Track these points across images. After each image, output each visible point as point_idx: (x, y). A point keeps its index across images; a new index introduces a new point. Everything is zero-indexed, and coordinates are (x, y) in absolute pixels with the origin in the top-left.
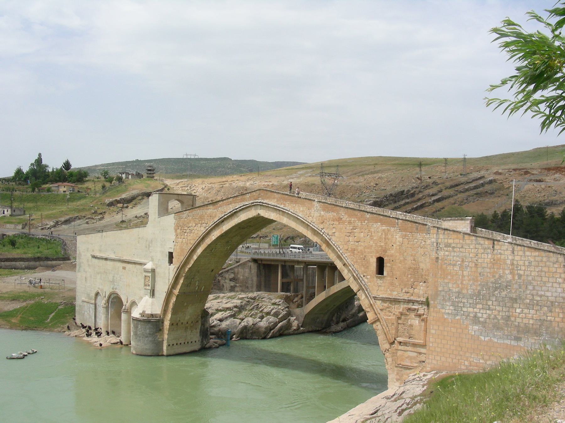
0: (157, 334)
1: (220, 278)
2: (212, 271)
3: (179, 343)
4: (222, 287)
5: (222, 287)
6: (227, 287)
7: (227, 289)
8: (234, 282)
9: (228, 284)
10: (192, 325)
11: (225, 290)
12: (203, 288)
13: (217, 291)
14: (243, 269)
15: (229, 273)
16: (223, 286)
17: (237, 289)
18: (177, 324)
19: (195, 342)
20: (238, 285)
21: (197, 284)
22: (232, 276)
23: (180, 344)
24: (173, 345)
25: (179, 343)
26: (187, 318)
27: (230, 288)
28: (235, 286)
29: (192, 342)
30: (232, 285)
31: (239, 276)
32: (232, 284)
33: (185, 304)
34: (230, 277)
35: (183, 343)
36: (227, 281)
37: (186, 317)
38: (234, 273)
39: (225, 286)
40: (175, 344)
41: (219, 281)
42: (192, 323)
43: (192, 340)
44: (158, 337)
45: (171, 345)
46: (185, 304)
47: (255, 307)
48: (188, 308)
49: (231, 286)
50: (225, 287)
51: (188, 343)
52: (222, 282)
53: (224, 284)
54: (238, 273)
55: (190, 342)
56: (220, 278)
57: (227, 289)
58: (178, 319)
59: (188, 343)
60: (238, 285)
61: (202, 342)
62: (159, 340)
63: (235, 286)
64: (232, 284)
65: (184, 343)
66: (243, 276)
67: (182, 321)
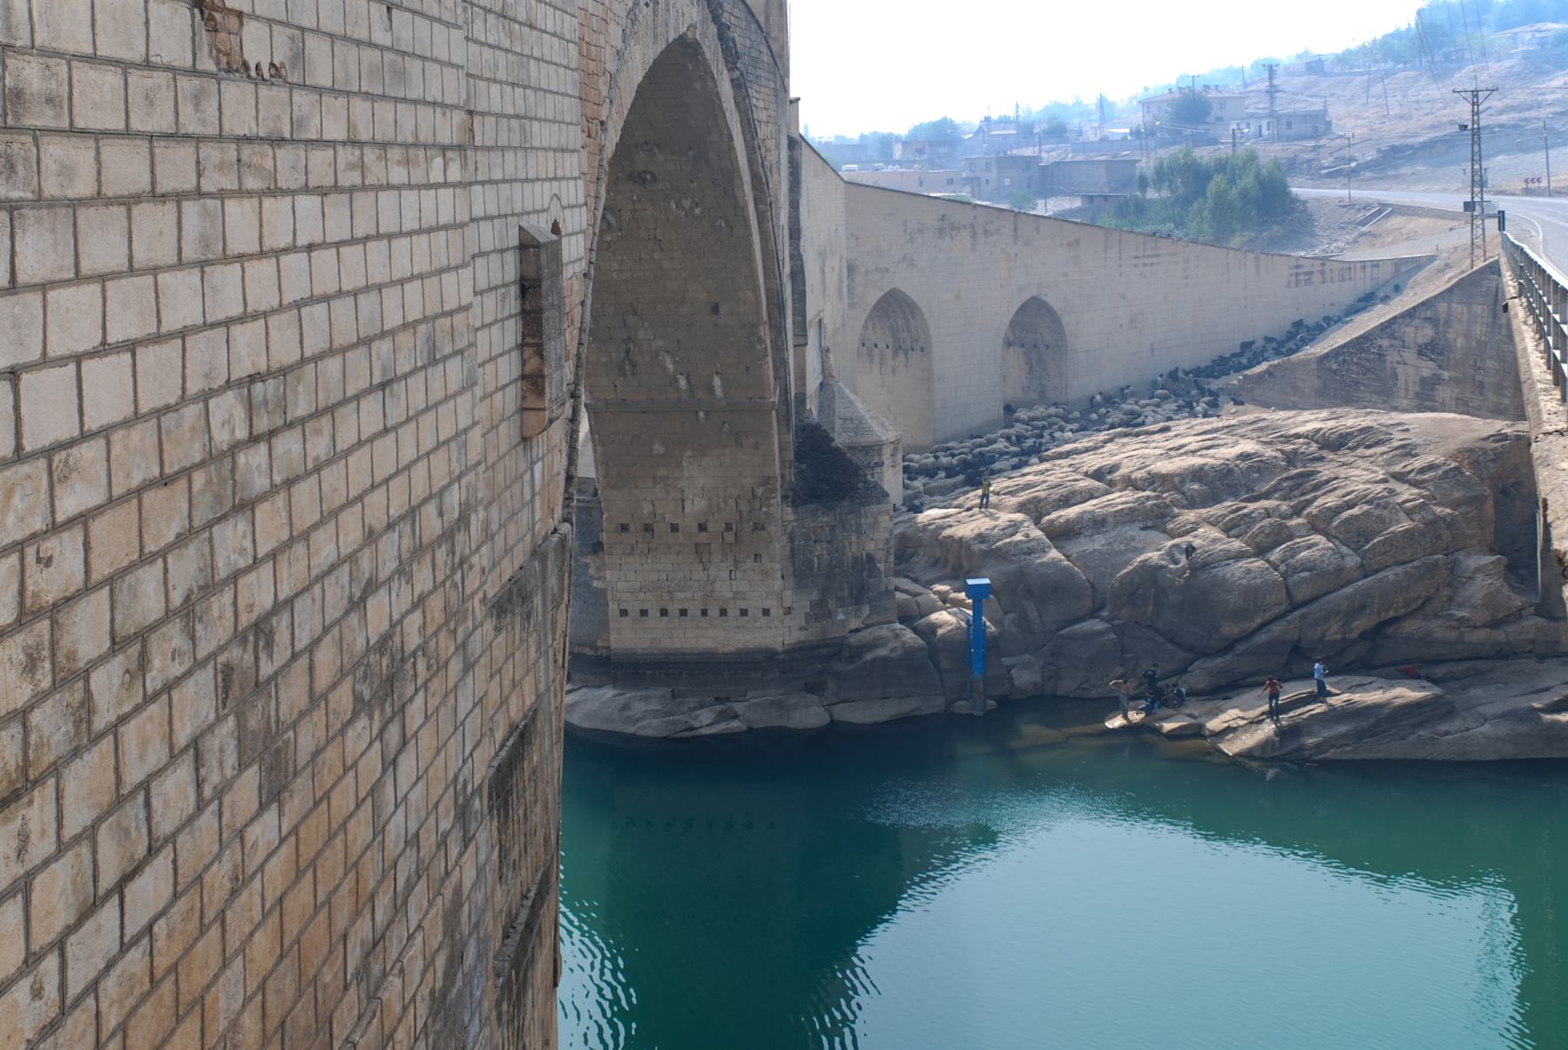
0: (588, 559)
1: (1385, 343)
2: (715, 309)
3: (674, 608)
4: (1391, 383)
5: (1391, 383)
6: (1407, 384)
7: (1407, 390)
8: (1431, 364)
9: (1411, 370)
10: (729, 537)
11: (1402, 394)
12: (717, 382)
13: (1374, 398)
14: (1469, 305)
15: (1416, 322)
16: (1395, 377)
17: (1444, 393)
18: (648, 528)
19: (766, 612)
20: (1446, 375)
21: (670, 367)
22: (1428, 333)
23: (683, 612)
24: (644, 613)
25: (674, 608)
26: (696, 506)
27: (1417, 389)
28: (1435, 381)
29: (744, 612)
30: (1426, 373)
31: (1451, 336)
32: (1427, 368)
33: (658, 448)
34: (1421, 340)
35: (694, 610)
36: (1410, 356)
37: (688, 504)
38: (1433, 321)
39: (1401, 377)
40: (654, 612)
41: (1381, 357)
42: (728, 527)
43: (742, 604)
44: (591, 571)
45: (634, 612)
46: (658, 448)
47: (1285, 484)
48: (679, 465)
49: (1423, 380)
50: (1401, 384)
51: (723, 612)
52: (1392, 358)
53: (1400, 368)
54: (1448, 323)
55: (733, 612)
56: (1385, 343)
57: (1407, 390)
58: (647, 508)
59: (723, 612)
60: (1446, 375)
61: (820, 611)
62: (595, 584)
63: (1435, 381)
64: (1427, 368)
65: (704, 613)
66: (1467, 336)
67: (669, 518)
